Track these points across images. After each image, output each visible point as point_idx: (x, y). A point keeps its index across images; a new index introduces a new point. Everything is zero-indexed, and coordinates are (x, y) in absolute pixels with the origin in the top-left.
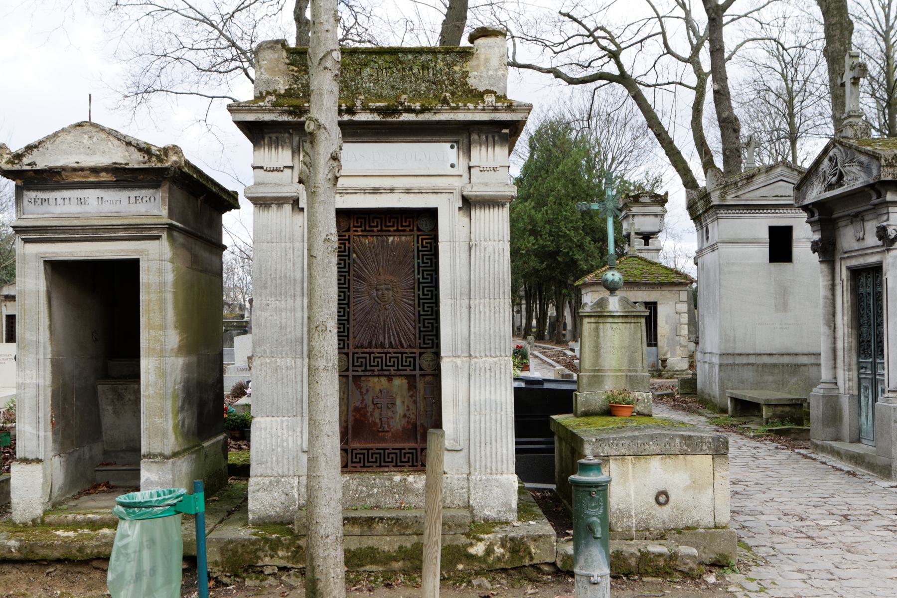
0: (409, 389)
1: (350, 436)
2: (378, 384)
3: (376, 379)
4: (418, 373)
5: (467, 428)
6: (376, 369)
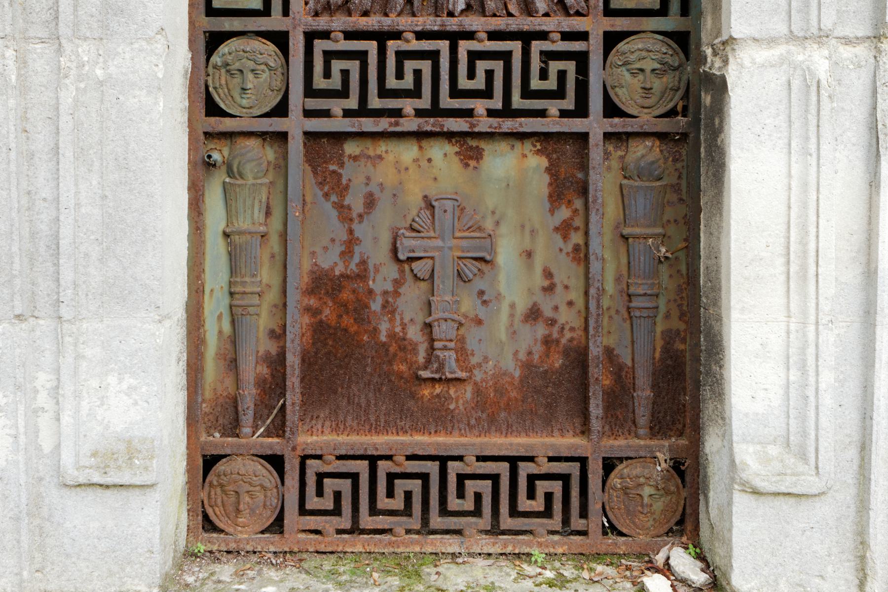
0: (556, 197)
1: (293, 397)
2: (412, 172)
3: (408, 152)
4: (595, 124)
5: (853, 387)
6: (408, 105)
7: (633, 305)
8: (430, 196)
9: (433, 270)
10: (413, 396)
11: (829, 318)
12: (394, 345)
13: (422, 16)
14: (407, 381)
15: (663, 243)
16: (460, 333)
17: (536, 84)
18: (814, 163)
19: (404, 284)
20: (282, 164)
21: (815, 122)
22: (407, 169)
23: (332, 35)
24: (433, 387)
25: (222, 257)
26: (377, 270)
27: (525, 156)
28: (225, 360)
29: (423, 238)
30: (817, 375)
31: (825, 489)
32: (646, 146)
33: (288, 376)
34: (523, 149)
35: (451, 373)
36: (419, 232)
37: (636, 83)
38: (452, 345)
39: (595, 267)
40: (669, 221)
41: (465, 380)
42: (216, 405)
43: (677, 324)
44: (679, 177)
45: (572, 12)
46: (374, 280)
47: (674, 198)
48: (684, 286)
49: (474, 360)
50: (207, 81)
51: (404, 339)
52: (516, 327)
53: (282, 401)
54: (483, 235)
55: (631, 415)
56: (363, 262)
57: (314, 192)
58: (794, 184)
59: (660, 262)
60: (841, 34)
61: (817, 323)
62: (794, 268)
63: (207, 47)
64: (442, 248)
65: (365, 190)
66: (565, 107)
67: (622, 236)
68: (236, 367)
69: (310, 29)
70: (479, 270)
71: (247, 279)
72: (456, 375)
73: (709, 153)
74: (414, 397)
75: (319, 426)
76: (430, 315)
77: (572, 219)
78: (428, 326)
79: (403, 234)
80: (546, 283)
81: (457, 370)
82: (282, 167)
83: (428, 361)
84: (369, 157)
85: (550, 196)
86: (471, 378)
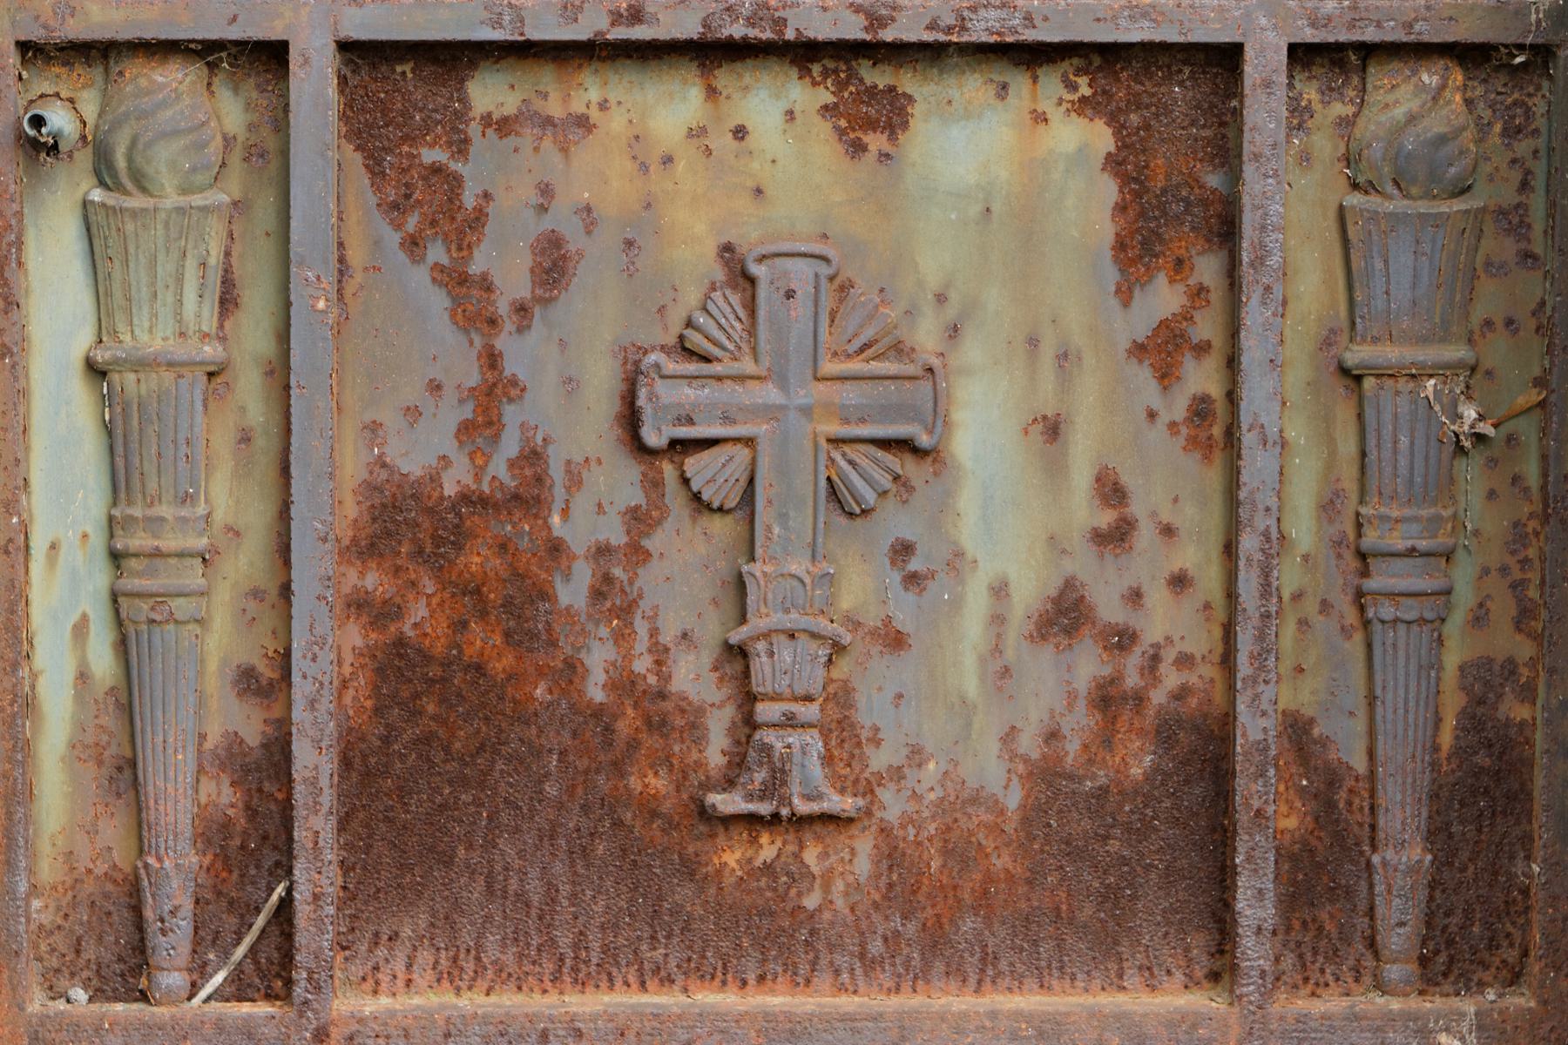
0: (1140, 246)
1: (316, 876)
7: (1372, 584)
8: (742, 248)
9: (751, 481)
10: (689, 869)
12: (630, 712)
14: (671, 825)
15: (1468, 393)
16: (835, 674)
19: (659, 522)
20: (271, 143)
22: (668, 160)
24: (754, 841)
26: (575, 481)
27: (1041, 118)
28: (100, 763)
29: (719, 378)
32: (1423, 87)
33: (300, 812)
34: (1034, 98)
35: (808, 798)
36: (706, 359)
38: (810, 712)
39: (1257, 465)
40: (1488, 323)
41: (851, 820)
42: (74, 904)
44: (1524, 186)
46: (565, 513)
47: (1508, 249)
48: (1533, 525)
49: (879, 760)
51: (662, 695)
52: (1010, 654)
53: (280, 890)
54: (910, 369)
55: (1362, 922)
56: (532, 457)
57: (372, 234)
59: (1460, 450)
64: (778, 410)
67: (1344, 371)
70: (896, 478)
71: (165, 510)
74: (692, 874)
75: (399, 966)
76: (743, 619)
77: (1187, 317)
79: (657, 366)
80: (1105, 519)
81: (826, 789)
82: (270, 152)
83: (738, 763)
84: (548, 122)
85: (1120, 246)
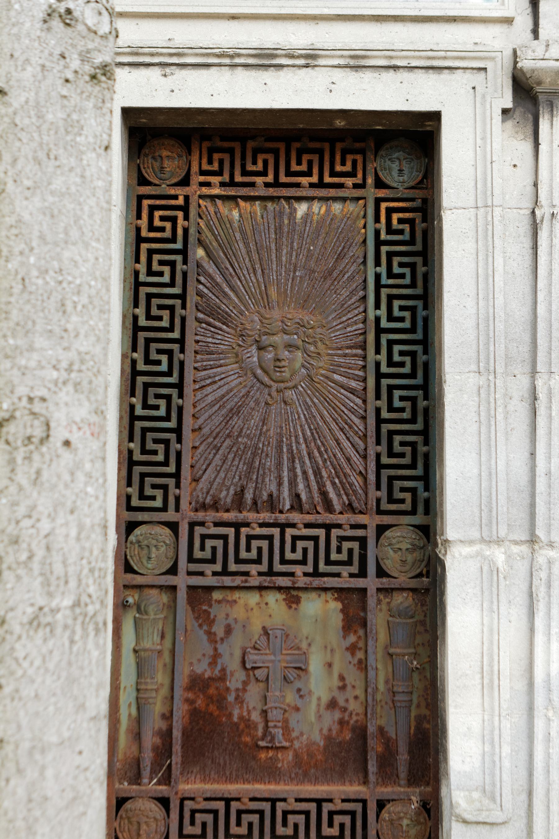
1: (176, 759)
2: (256, 611)
3: (253, 598)
4: (371, 582)
5: (523, 756)
6: (253, 569)
7: (396, 698)
10: (254, 758)
11: (507, 712)
13: (263, 512)
15: (415, 659)
17: (334, 556)
18: (496, 617)
20: (172, 604)
21: (496, 592)
23: (206, 524)
24: (268, 752)
25: (134, 668)
26: (232, 675)
27: (327, 601)
28: (132, 733)
29: (262, 654)
30: (500, 748)
31: (506, 819)
32: (403, 596)
33: (174, 745)
36: (259, 650)
37: (397, 557)
38: (280, 724)
39: (371, 674)
40: (418, 644)
42: (125, 764)
43: (424, 711)
44: (425, 616)
45: (357, 512)
46: (230, 681)
47: (422, 629)
48: (429, 686)
49: (294, 735)
50: (126, 552)
51: (249, 720)
52: (321, 713)
53: (169, 762)
55: (395, 771)
56: (223, 670)
57: (192, 624)
58: (485, 630)
59: (413, 670)
60: (512, 539)
61: (500, 716)
62: (486, 681)
63: (126, 530)
64: (273, 661)
65: (225, 622)
66: (352, 572)
67: (389, 654)
68: (140, 738)
69: (192, 520)
71: (148, 680)
72: (283, 745)
73: (440, 603)
75: (193, 778)
76: (266, 704)
77: (357, 642)
78: (264, 713)
80: (341, 684)
81: (283, 741)
82: (173, 606)
85: (343, 627)
86: (292, 746)
